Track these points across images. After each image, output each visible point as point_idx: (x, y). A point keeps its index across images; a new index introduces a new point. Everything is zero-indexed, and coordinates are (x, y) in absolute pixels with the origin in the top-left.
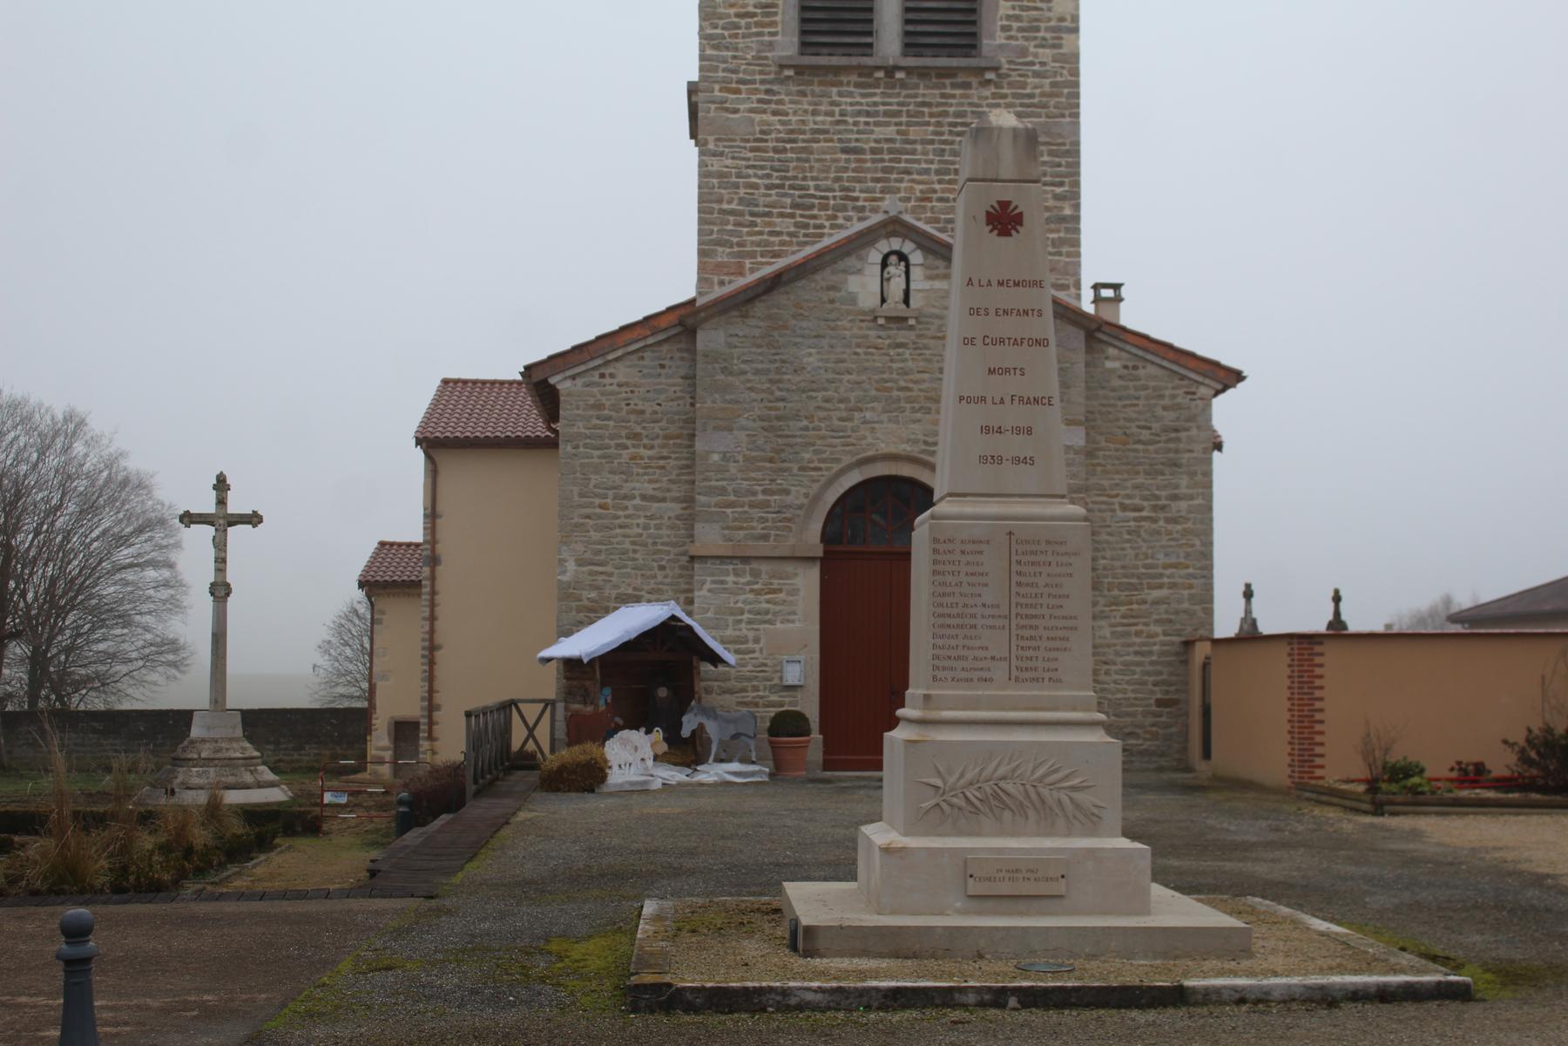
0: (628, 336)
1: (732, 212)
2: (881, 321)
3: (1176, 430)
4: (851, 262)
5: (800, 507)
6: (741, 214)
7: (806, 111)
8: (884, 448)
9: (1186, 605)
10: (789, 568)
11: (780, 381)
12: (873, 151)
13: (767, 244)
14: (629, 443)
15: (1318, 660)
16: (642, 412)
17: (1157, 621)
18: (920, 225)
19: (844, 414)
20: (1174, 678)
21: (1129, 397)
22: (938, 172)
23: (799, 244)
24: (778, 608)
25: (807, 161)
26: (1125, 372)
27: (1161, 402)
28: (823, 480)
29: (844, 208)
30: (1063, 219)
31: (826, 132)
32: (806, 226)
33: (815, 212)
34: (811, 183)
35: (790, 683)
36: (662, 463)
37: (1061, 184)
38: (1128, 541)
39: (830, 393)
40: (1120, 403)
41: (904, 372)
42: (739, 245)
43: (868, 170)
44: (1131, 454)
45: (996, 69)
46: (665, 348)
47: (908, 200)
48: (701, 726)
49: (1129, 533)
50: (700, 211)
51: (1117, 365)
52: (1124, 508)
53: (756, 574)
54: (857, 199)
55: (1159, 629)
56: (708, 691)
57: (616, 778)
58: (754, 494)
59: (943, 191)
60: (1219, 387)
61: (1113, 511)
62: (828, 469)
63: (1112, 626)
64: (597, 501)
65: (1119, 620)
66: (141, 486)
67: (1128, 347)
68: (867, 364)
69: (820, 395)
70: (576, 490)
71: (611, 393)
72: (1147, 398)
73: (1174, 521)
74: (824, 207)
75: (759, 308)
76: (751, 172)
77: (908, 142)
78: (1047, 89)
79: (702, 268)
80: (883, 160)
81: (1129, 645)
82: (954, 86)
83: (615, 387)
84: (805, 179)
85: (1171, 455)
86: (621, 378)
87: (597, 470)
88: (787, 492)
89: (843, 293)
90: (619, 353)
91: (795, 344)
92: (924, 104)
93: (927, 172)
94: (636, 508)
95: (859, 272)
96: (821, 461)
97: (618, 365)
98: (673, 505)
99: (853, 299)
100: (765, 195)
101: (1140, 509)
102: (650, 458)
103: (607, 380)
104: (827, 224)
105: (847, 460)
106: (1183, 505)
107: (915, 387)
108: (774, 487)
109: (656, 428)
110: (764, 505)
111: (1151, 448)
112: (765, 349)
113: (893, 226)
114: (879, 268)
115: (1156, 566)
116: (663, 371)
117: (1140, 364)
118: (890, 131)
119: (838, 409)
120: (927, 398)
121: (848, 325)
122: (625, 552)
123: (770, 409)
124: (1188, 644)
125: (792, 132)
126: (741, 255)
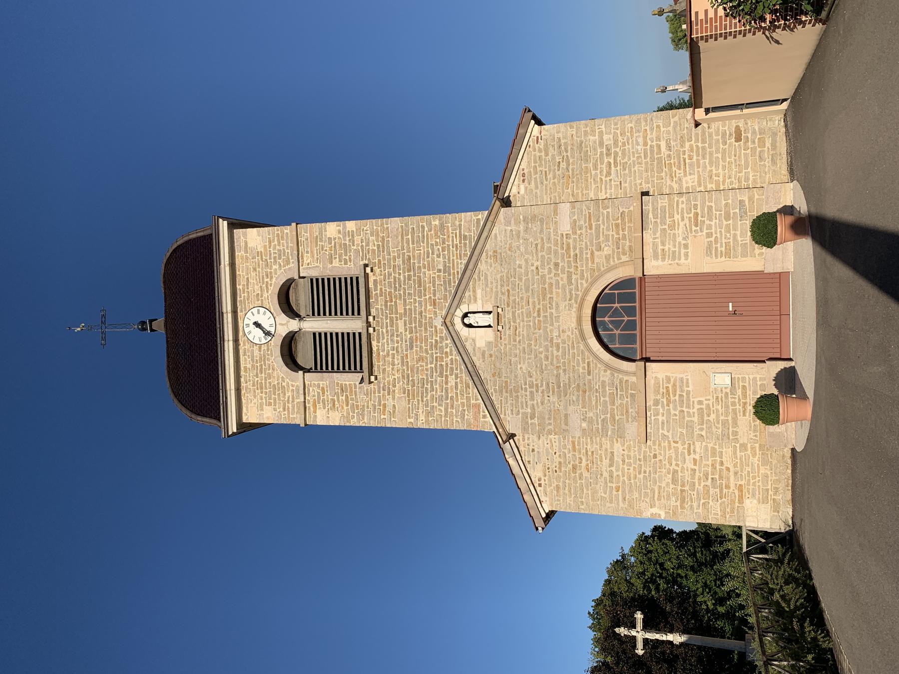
1: (446, 410)
4: (468, 345)
7: (393, 369)
8: (574, 325)
12: (411, 332)
13: (462, 391)
14: (578, 472)
16: (560, 463)
17: (682, 146)
25: (418, 368)
31: (402, 357)
32: (452, 369)
34: (429, 366)
36: (590, 453)
37: (423, 227)
39: (543, 356)
40: (545, 182)
41: (529, 315)
42: (463, 406)
45: (366, 266)
47: (435, 313)
51: (522, 187)
52: (609, 174)
54: (436, 341)
55: (687, 144)
60: (533, 122)
69: (544, 362)
70: (608, 505)
71: (550, 480)
77: (405, 314)
78: (374, 238)
80: (415, 327)
82: (376, 290)
83: (546, 478)
87: (595, 492)
92: (386, 306)
93: (420, 303)
94: (617, 471)
95: (474, 340)
99: (489, 344)
103: (542, 482)
104: (450, 357)
106: (605, 137)
107: (537, 306)
116: (536, 450)
118: (401, 323)
119: (552, 351)
120: (544, 299)
125: (403, 377)
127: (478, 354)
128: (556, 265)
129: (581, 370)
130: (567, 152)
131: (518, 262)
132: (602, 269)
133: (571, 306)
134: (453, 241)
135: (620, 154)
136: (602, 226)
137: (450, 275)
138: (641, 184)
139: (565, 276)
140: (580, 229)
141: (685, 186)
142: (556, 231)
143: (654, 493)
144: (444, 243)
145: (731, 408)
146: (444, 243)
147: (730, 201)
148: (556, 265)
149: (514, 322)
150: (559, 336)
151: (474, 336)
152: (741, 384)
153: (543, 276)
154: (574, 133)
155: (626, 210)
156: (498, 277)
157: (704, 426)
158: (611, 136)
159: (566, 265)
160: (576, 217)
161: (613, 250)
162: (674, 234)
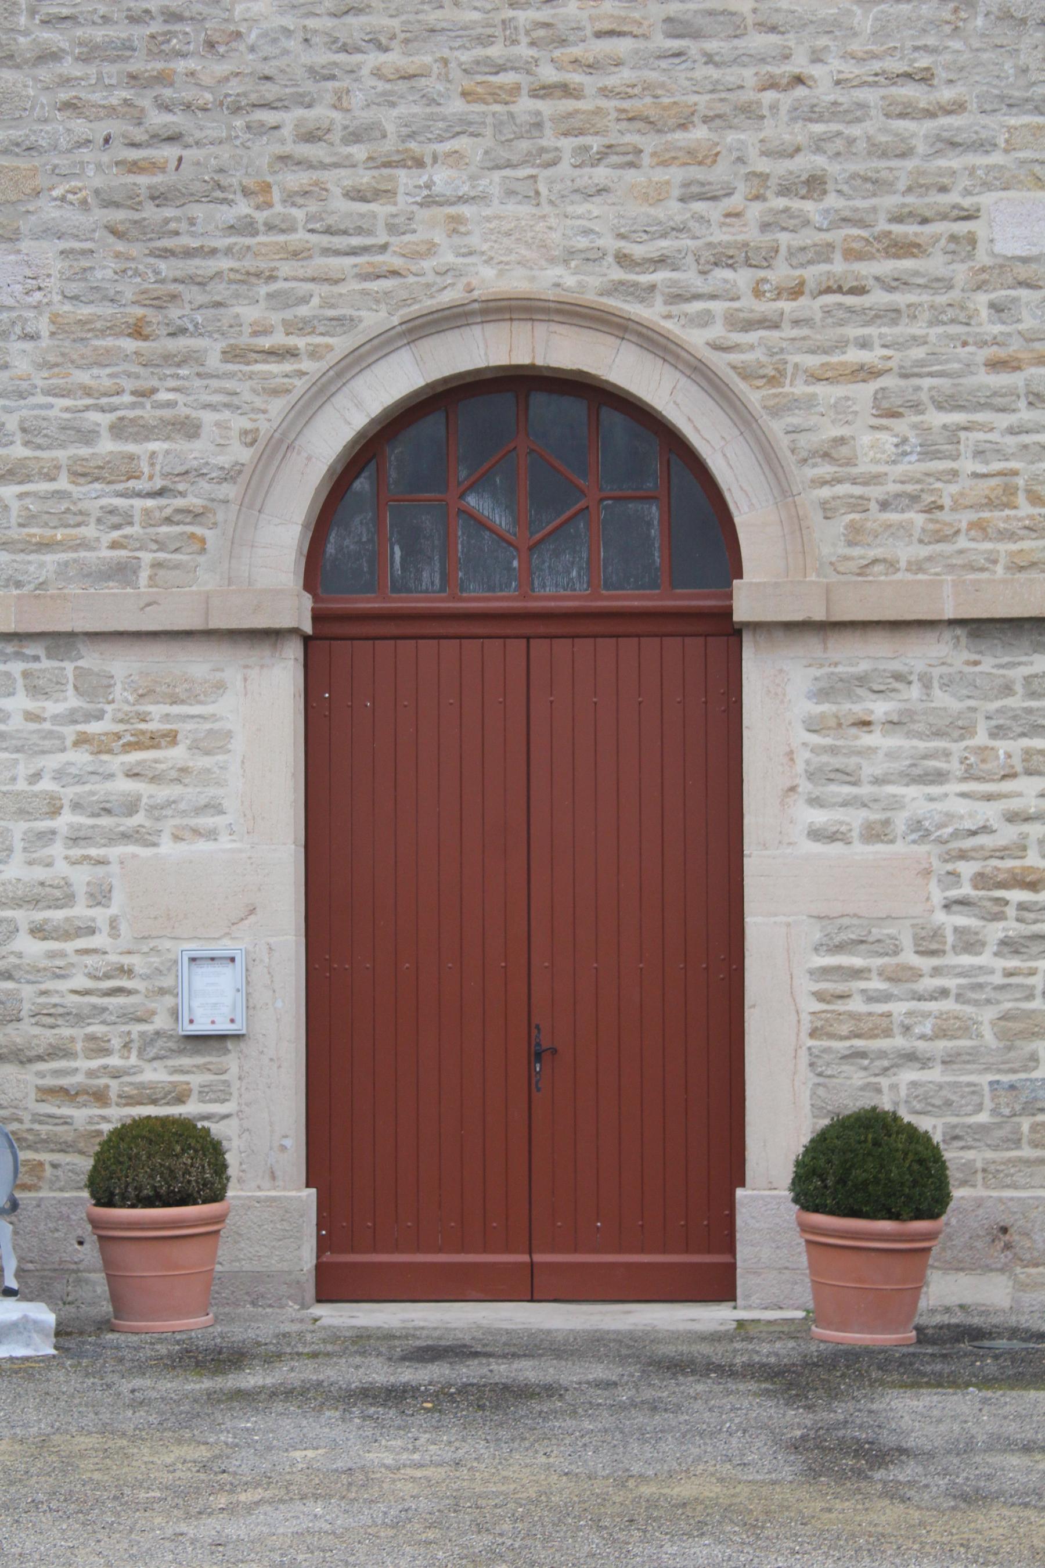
5: (229, 476)
8: (490, 280)
10: (197, 664)
11: (162, 79)
19: (365, 178)
24: (163, 793)
28: (300, 385)
35: (202, 1026)
39: (321, 113)
53: (96, 688)
58: (88, 436)
62: (314, 354)
69: (289, 119)
88: (190, 429)
96: (294, 327)
105: (375, 320)
108: (147, 413)
123: (134, 167)
128: (814, 185)
129: (250, 313)
133: (593, 258)
136: (1004, 420)
139: (751, 234)
140: (996, 308)
142: (1000, 181)
145: (78, 1032)
148: (814, 185)
150: (430, 202)
152: (196, 1080)
153: (750, 112)
159: (807, 237)
161: (875, 479)
162: (939, 777)
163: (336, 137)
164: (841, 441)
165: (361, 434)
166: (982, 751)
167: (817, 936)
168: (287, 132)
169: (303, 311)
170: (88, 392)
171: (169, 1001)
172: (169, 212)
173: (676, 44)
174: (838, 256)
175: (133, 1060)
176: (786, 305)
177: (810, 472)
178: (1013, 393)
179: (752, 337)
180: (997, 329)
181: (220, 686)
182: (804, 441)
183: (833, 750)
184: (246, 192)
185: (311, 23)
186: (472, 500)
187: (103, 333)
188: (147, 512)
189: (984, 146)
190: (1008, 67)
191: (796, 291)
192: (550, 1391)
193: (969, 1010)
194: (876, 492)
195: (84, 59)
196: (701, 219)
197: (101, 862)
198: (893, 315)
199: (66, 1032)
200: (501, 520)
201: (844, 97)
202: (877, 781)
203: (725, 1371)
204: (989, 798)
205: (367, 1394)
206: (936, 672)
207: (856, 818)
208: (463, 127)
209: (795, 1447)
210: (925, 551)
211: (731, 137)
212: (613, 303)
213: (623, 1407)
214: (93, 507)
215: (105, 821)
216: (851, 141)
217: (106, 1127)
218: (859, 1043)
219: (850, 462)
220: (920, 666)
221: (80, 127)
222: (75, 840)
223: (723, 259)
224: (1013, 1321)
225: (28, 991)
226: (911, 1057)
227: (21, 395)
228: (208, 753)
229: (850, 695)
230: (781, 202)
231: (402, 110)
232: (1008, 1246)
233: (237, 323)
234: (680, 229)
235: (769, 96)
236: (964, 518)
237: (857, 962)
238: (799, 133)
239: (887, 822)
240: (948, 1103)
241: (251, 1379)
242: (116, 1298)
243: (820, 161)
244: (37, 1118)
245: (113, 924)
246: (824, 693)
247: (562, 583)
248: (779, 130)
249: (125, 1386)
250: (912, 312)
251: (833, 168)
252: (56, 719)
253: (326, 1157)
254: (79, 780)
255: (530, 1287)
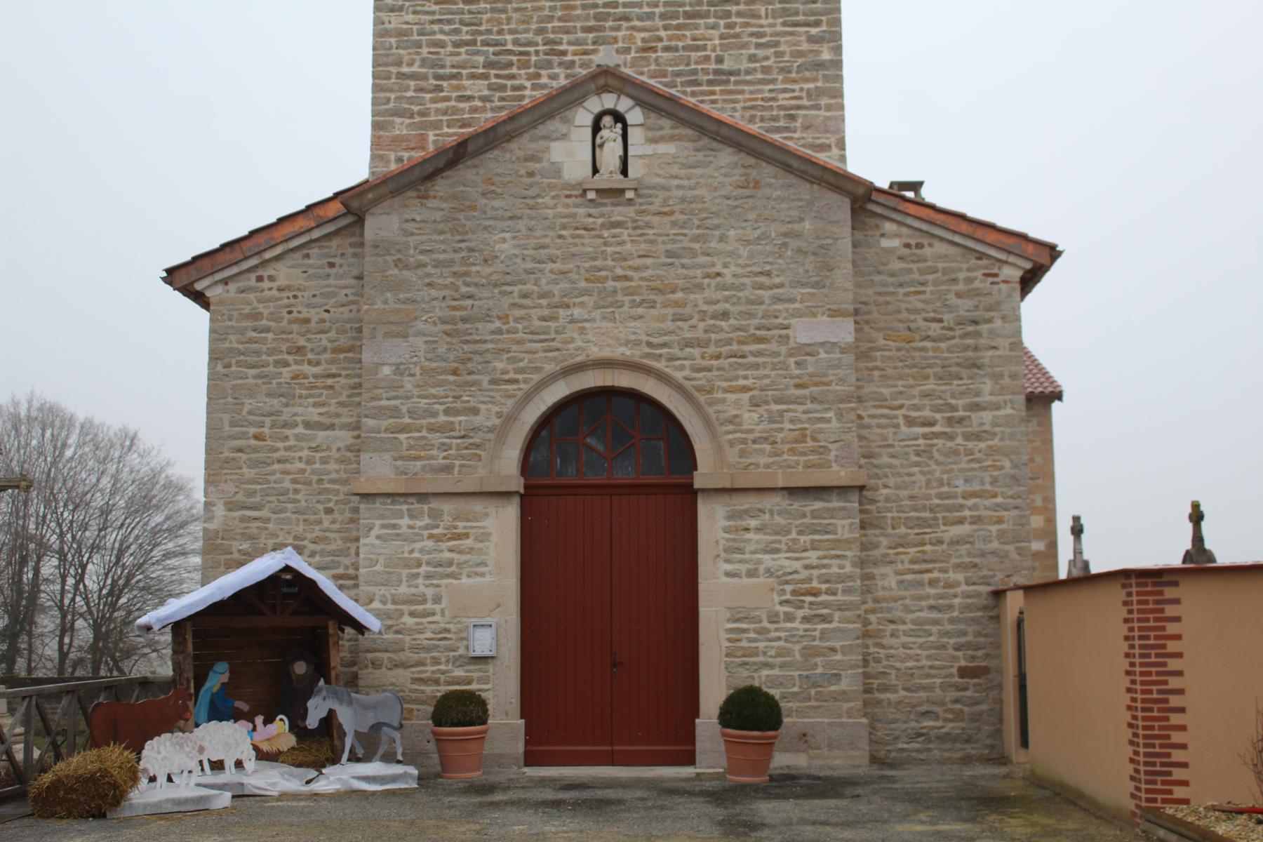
0: (288, 229)
1: (413, 76)
2: (591, 195)
3: (975, 322)
4: (555, 125)
5: (491, 430)
6: (424, 77)
8: (596, 352)
9: (995, 545)
10: (477, 506)
11: (466, 274)
13: (455, 111)
14: (290, 358)
15: (1170, 611)
16: (307, 321)
18: (644, 78)
19: (546, 312)
20: (982, 640)
21: (912, 283)
22: (663, 16)
23: (492, 109)
25: (504, 11)
26: (907, 251)
27: (955, 288)
28: (520, 394)
29: (549, 65)
30: (820, 65)
32: (502, 88)
33: (514, 71)
34: (509, 38)
35: (478, 653)
36: (330, 382)
37: (817, 24)
38: (917, 464)
39: (529, 287)
40: (901, 291)
42: (422, 114)
43: (578, 18)
44: (917, 354)
46: (335, 243)
47: (627, 51)
48: (331, 712)
49: (918, 455)
50: (375, 76)
52: (910, 422)
53: (436, 515)
54: (564, 53)
55: (960, 577)
56: (376, 665)
57: (143, 796)
59: (670, 38)
60: (1028, 266)
61: (897, 426)
62: (525, 381)
63: (898, 573)
64: (252, 430)
65: (907, 566)
66: (180, 489)
67: (909, 221)
68: (573, 250)
69: (516, 289)
71: (270, 300)
72: (935, 283)
73: (978, 437)
74: (524, 65)
75: (441, 186)
76: (436, 27)
79: (376, 143)
81: (921, 598)
83: (274, 292)
84: (500, 32)
85: (970, 354)
86: (282, 282)
87: (252, 393)
88: (475, 411)
89: (545, 164)
90: (278, 250)
91: (485, 228)
93: (650, 16)
95: (564, 137)
96: (516, 371)
97: (279, 265)
98: (343, 433)
99: (557, 170)
100: (452, 54)
101: (931, 424)
102: (315, 376)
104: (528, 84)
105: (550, 368)
106: (987, 416)
108: (458, 405)
109: (324, 340)
110: (446, 429)
111: (943, 345)
112: (448, 236)
113: (607, 79)
114: (588, 132)
115: (955, 496)
117: (925, 241)
121: (552, 203)
122: (284, 493)
123: (455, 308)
124: (998, 594)
126: (422, 126)
127: (533, 146)
128: (725, 315)
129: (500, 365)
130: (962, 337)
131: (732, 233)
132: (711, 410)
134: (785, 91)
135: (950, 444)
136: (801, 408)
137: (710, 83)
138: (886, 486)
140: (798, 364)
141: (876, 571)
142: (798, 314)
143: (255, 508)
144: (781, 70)
146: (781, 70)
147: (839, 657)
148: (725, 315)
149: (603, 226)
150: (571, 322)
151: (573, 136)
152: (476, 675)
153: (699, 287)
154: (999, 353)
155: (832, 456)
156: (702, 192)
157: (390, 606)
158: (987, 428)
159: (722, 336)
160: (823, 355)
161: (750, 431)
162: (777, 551)
163: (535, 296)
164: (736, 416)
165: (544, 414)
166: (794, 540)
167: (728, 615)
168: (515, 294)
169: (521, 364)
170: (434, 397)
171: (465, 642)
172: (468, 326)
173: (670, 260)
174: (735, 343)
175: (450, 667)
176: (714, 362)
177: (725, 429)
178: (804, 397)
179: (701, 375)
180: (798, 372)
181: (487, 515)
182: (722, 416)
183: (734, 540)
184: (499, 318)
185: (526, 252)
186: (588, 440)
187: (441, 374)
188: (458, 445)
189: (792, 300)
190: (801, 270)
191: (718, 357)
192: (620, 801)
193: (790, 645)
194: (751, 436)
195: (436, 267)
196: (680, 328)
197: (438, 586)
198: (757, 366)
199: (423, 655)
200: (600, 448)
201: (736, 281)
202: (753, 553)
203: (692, 793)
204: (797, 559)
205: (545, 803)
206: (776, 508)
207: (743, 568)
208: (586, 292)
209: (720, 823)
210: (771, 460)
211: (692, 296)
212: (646, 361)
213: (649, 808)
214: (437, 442)
215: (440, 569)
216: (739, 298)
217: (439, 694)
218: (746, 659)
219: (740, 424)
220: (769, 506)
221: (433, 293)
222: (427, 577)
223: (689, 344)
224: (808, 772)
225: (407, 638)
226: (767, 665)
227: (408, 398)
228: (481, 541)
229: (741, 518)
230: (712, 322)
231: (562, 286)
232: (806, 742)
233: (494, 369)
234: (672, 332)
235: (706, 281)
236: (786, 447)
237: (744, 626)
238: (719, 295)
239: (756, 569)
240: (782, 683)
241: (498, 797)
242: (443, 764)
243: (727, 306)
244: (411, 691)
245: (443, 611)
246: (730, 517)
247: (625, 473)
248: (710, 294)
249: (446, 800)
250: (764, 365)
251: (733, 309)
252: (420, 528)
253: (529, 705)
254: (429, 553)
255: (611, 760)
